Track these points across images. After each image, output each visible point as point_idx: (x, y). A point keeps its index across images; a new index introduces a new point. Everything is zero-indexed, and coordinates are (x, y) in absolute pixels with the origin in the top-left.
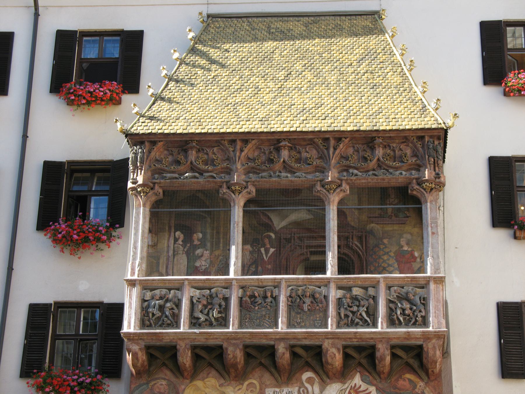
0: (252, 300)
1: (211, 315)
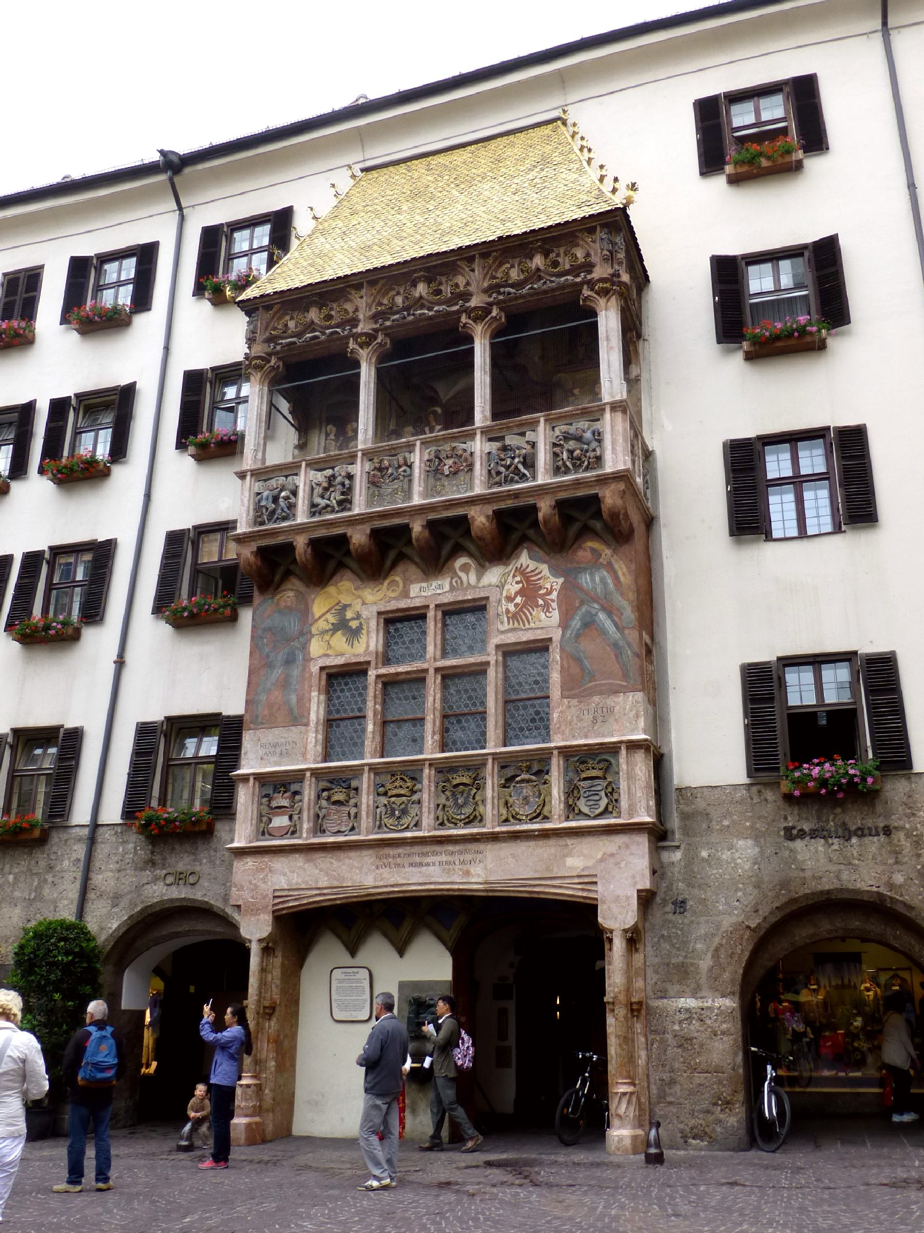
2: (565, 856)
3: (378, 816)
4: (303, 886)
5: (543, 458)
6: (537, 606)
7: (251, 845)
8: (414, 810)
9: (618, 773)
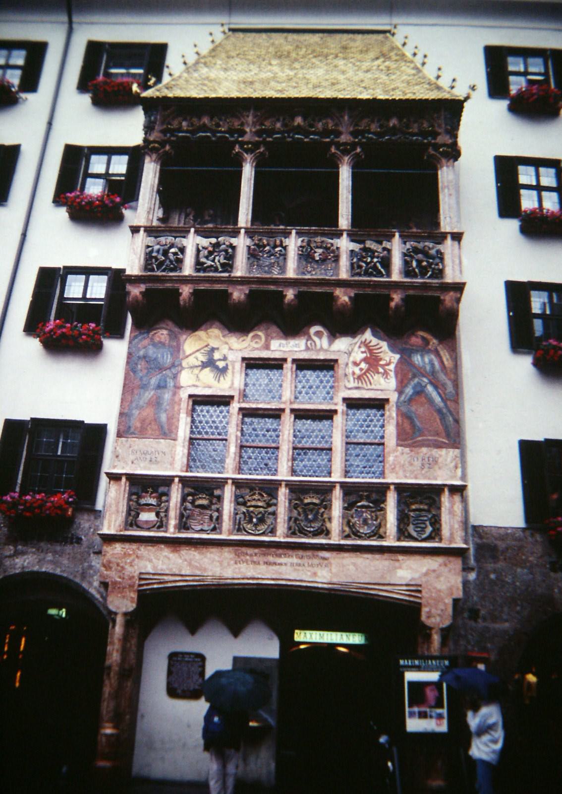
0: (261, 249)
1: (216, 261)
2: (396, 568)
3: (237, 521)
4: (167, 572)
5: (397, 262)
6: (378, 373)
7: (122, 533)
8: (269, 521)
9: (439, 508)
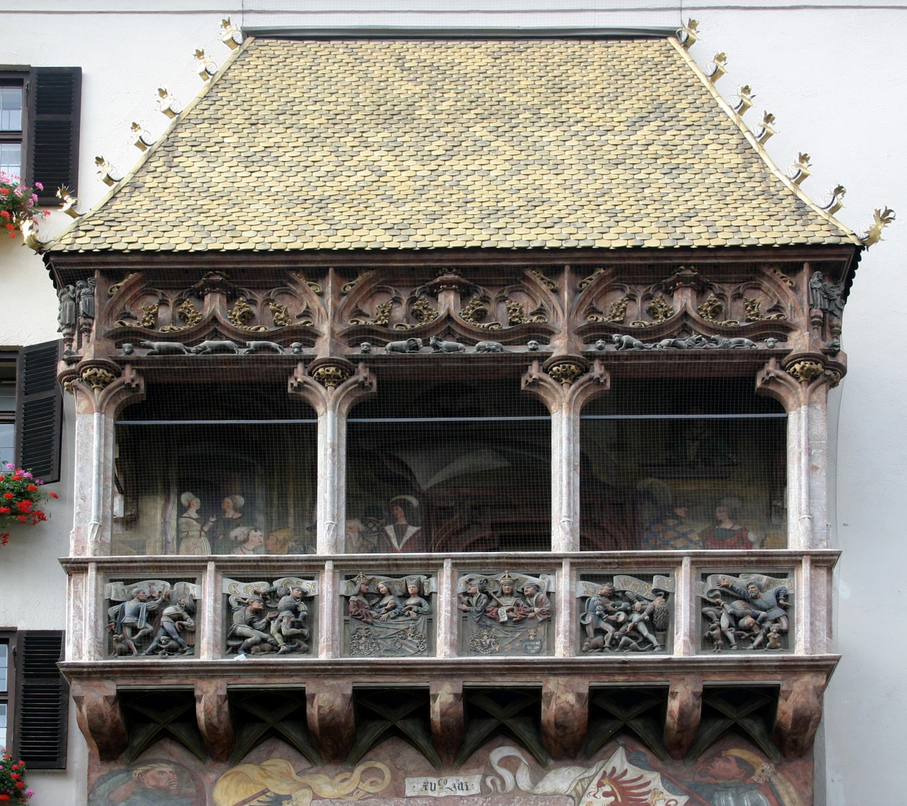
0: (374, 602)
